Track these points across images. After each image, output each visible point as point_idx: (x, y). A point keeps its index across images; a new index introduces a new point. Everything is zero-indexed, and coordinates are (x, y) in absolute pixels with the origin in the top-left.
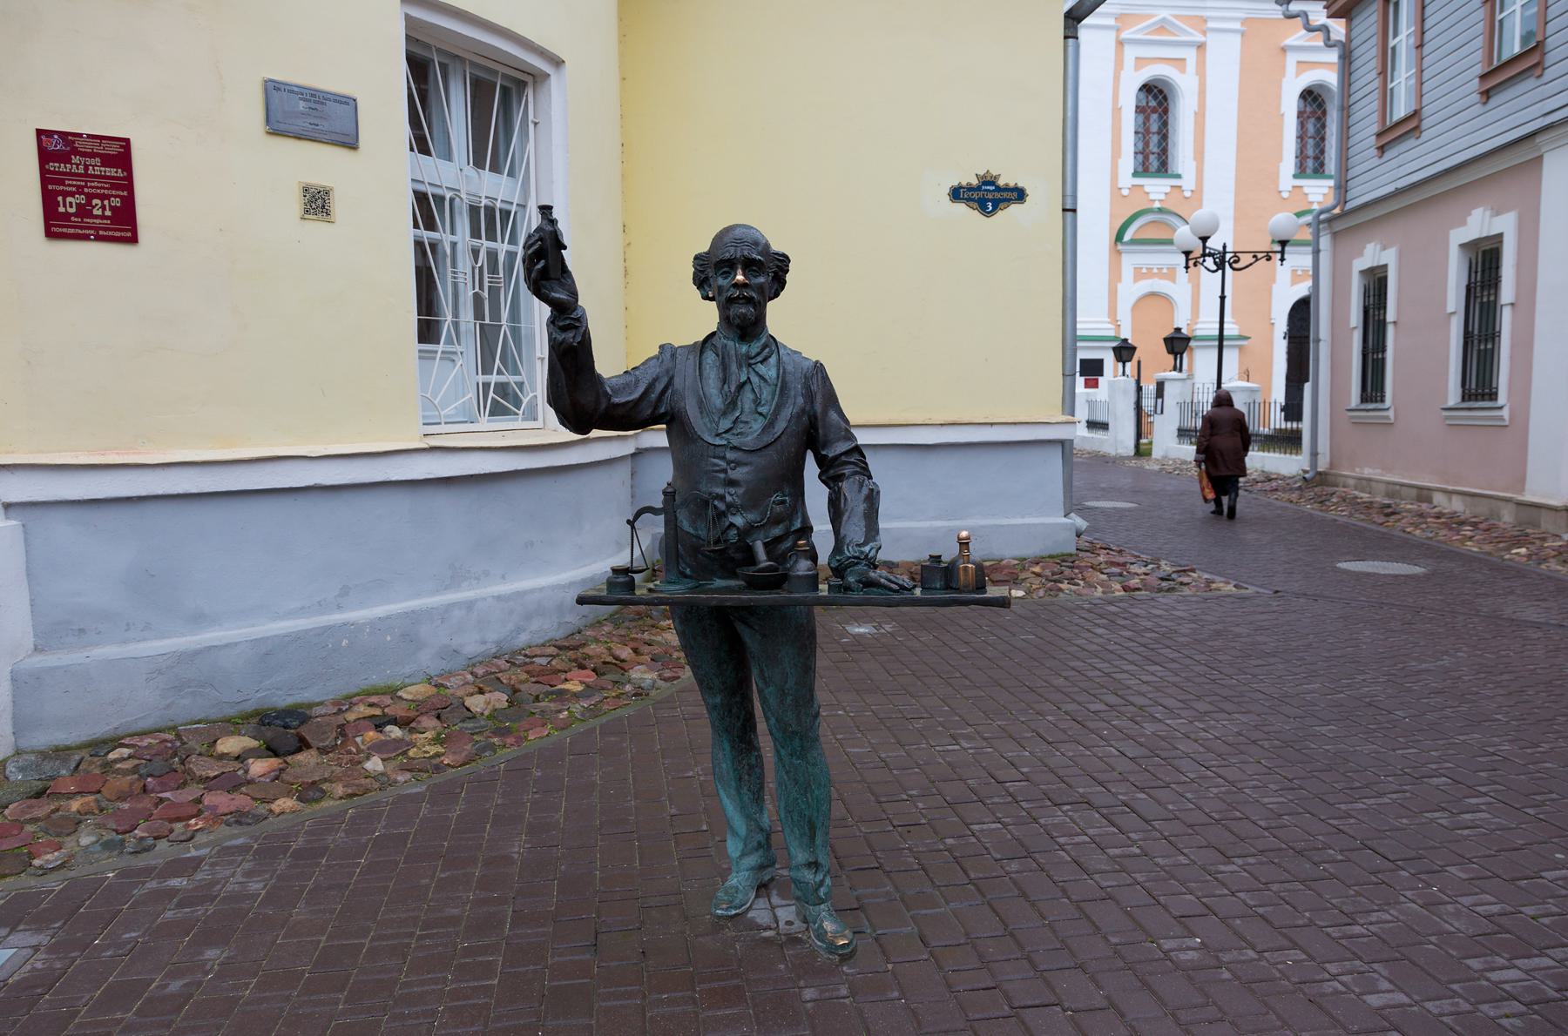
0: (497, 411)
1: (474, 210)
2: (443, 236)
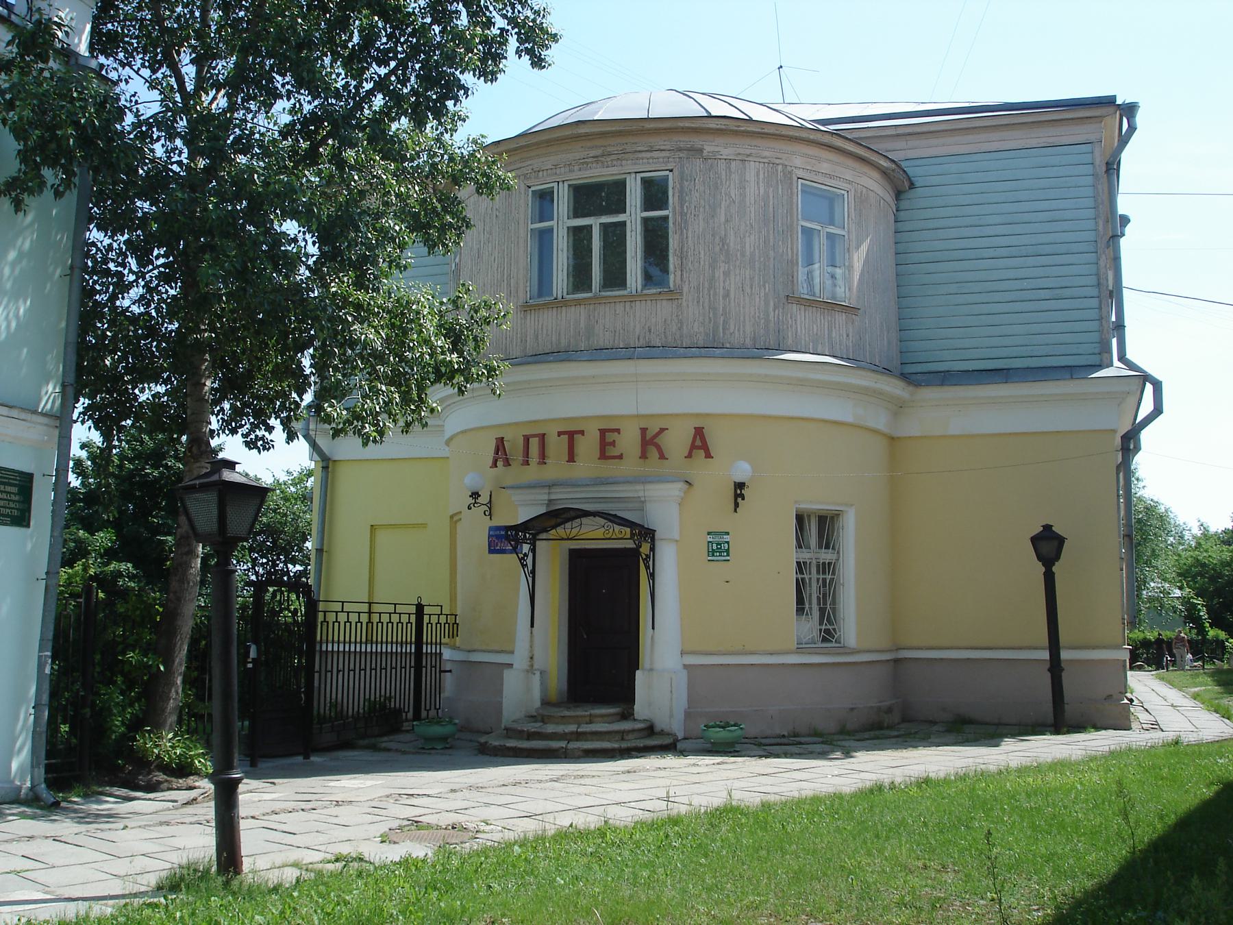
0: (824, 640)
1: (818, 566)
2: (806, 577)
